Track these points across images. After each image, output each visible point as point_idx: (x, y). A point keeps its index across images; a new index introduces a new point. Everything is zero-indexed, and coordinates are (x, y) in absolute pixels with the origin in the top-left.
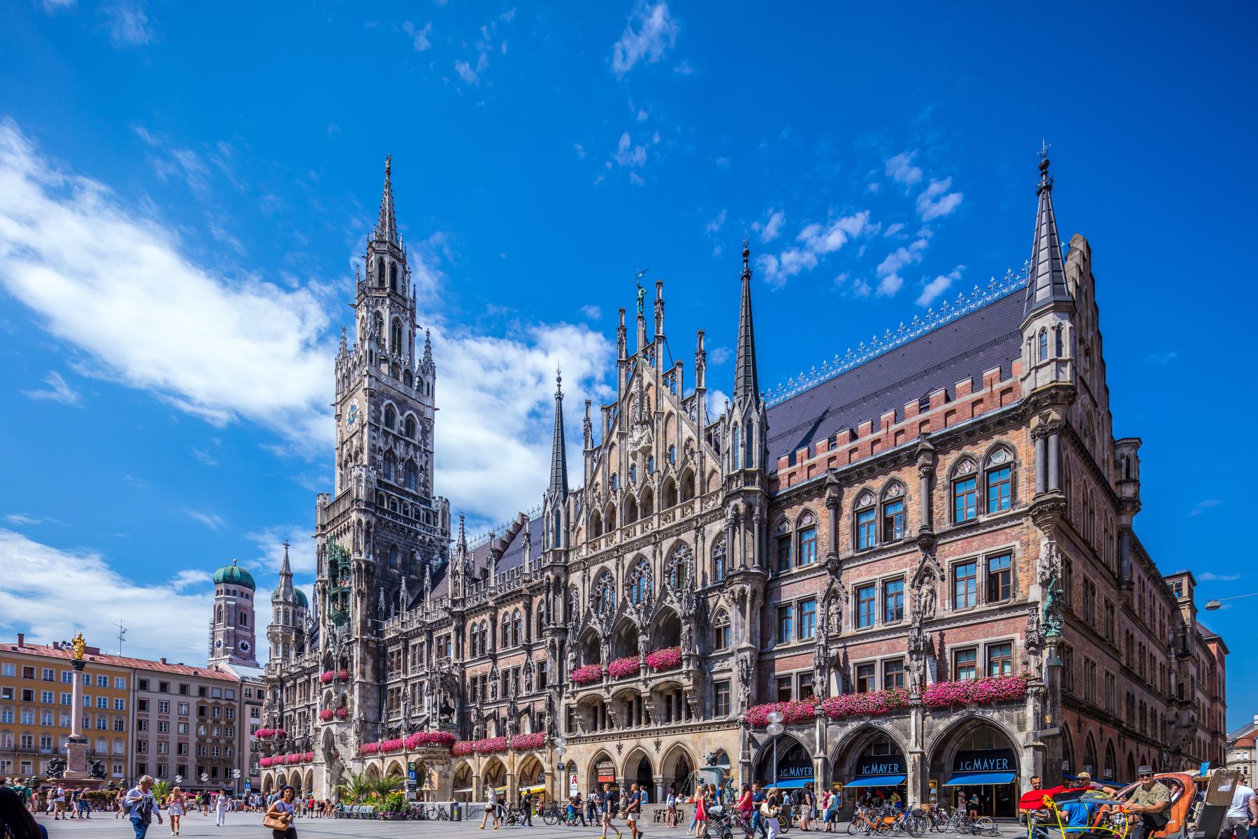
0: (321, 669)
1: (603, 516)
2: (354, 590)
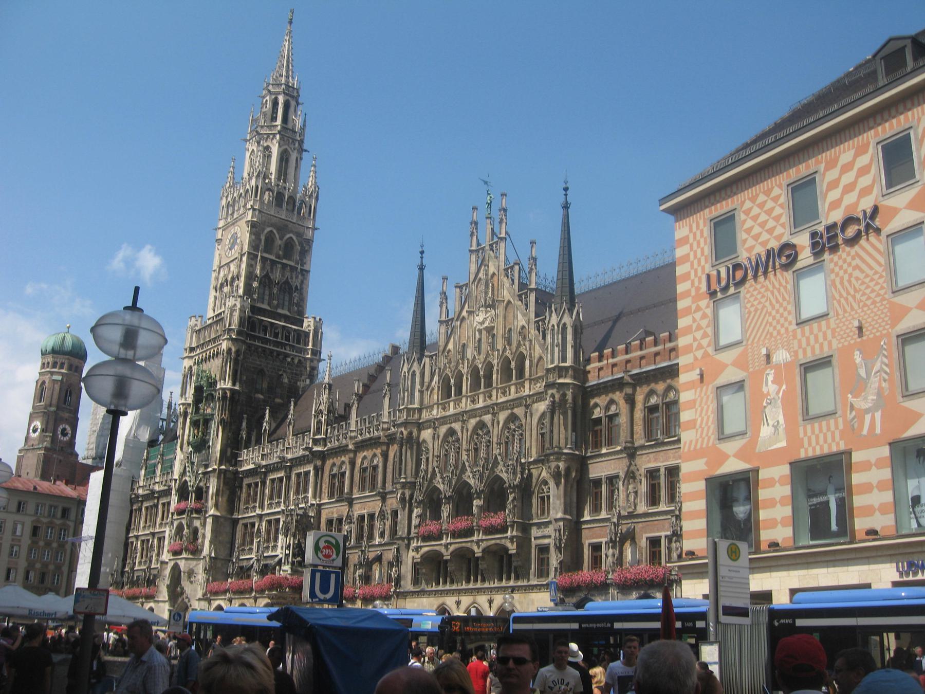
1: (452, 381)
2: (217, 419)
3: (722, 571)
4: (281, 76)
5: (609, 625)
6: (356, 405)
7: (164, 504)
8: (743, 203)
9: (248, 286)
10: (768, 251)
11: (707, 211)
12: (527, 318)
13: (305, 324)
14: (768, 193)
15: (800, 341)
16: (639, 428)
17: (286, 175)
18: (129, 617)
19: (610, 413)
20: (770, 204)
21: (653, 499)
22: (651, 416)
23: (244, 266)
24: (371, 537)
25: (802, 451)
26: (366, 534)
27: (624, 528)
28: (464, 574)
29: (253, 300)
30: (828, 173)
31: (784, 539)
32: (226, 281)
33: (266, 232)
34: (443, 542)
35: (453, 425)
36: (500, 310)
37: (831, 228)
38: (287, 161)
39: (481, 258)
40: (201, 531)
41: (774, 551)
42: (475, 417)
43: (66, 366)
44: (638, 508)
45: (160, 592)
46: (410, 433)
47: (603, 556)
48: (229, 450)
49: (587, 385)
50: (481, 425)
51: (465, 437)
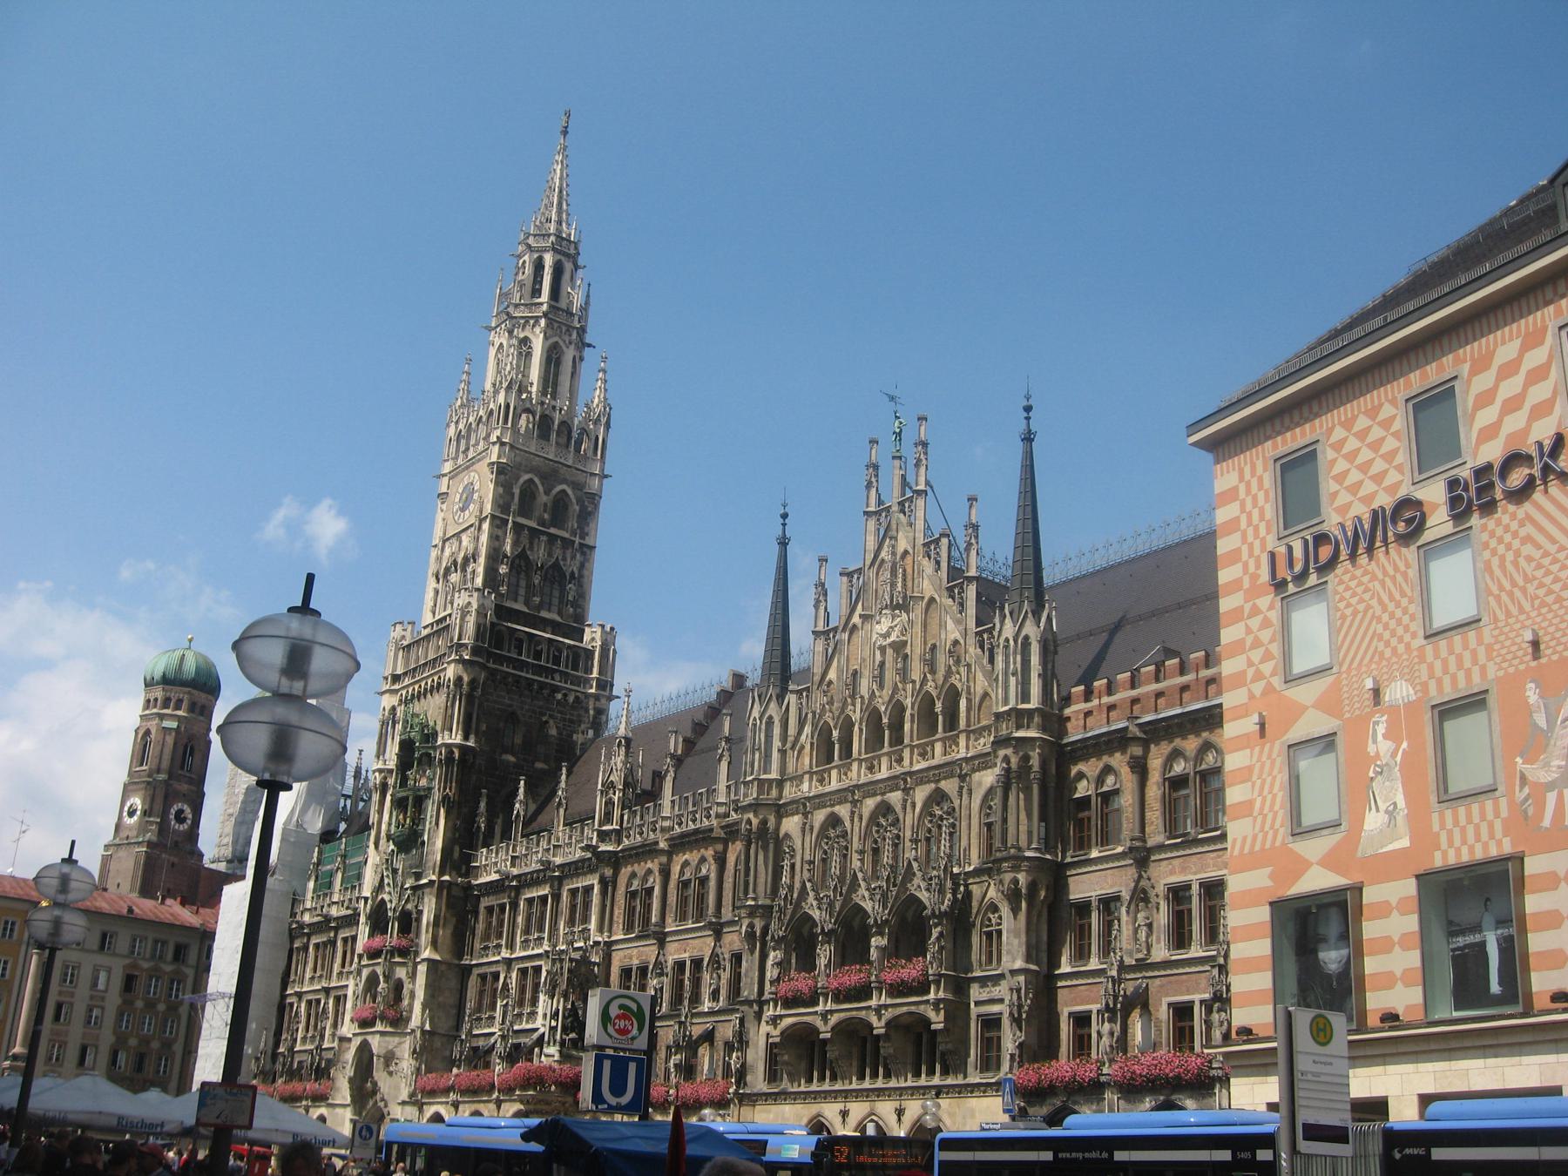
0: (363, 931)
1: (835, 733)
2: (436, 795)
3: (1302, 1064)
4: (549, 220)
5: (1105, 1155)
6: (671, 774)
7: (345, 940)
8: (1330, 431)
9: (491, 572)
10: (1375, 512)
11: (1269, 443)
12: (962, 628)
13: (587, 637)
14: (1372, 413)
15: (1431, 667)
16: (1155, 816)
17: (555, 385)
18: (284, 1132)
19: (1105, 789)
20: (1377, 432)
21: (1180, 937)
22: (1175, 795)
23: (484, 538)
24: (696, 999)
25: (1438, 855)
26: (687, 995)
27: (1130, 987)
28: (855, 1063)
29: (499, 595)
30: (1475, 379)
31: (1407, 1007)
32: (455, 563)
33: (522, 481)
34: (820, 1008)
35: (837, 809)
36: (917, 613)
37: (1482, 472)
38: (558, 363)
39: (884, 525)
40: (407, 987)
41: (1392, 1029)
42: (875, 795)
43: (185, 705)
44: (1153, 952)
45: (338, 1090)
46: (764, 822)
47: (1094, 1035)
48: (457, 848)
49: (1065, 741)
50: (885, 809)
51: (856, 829)
